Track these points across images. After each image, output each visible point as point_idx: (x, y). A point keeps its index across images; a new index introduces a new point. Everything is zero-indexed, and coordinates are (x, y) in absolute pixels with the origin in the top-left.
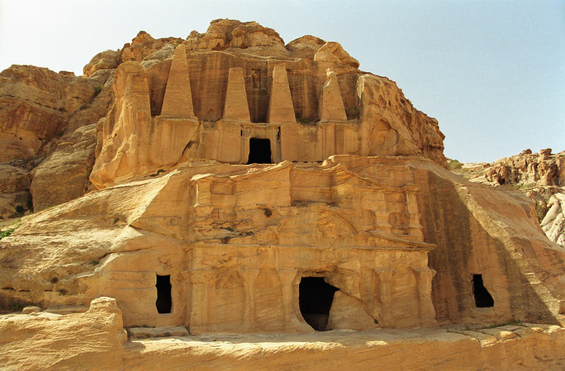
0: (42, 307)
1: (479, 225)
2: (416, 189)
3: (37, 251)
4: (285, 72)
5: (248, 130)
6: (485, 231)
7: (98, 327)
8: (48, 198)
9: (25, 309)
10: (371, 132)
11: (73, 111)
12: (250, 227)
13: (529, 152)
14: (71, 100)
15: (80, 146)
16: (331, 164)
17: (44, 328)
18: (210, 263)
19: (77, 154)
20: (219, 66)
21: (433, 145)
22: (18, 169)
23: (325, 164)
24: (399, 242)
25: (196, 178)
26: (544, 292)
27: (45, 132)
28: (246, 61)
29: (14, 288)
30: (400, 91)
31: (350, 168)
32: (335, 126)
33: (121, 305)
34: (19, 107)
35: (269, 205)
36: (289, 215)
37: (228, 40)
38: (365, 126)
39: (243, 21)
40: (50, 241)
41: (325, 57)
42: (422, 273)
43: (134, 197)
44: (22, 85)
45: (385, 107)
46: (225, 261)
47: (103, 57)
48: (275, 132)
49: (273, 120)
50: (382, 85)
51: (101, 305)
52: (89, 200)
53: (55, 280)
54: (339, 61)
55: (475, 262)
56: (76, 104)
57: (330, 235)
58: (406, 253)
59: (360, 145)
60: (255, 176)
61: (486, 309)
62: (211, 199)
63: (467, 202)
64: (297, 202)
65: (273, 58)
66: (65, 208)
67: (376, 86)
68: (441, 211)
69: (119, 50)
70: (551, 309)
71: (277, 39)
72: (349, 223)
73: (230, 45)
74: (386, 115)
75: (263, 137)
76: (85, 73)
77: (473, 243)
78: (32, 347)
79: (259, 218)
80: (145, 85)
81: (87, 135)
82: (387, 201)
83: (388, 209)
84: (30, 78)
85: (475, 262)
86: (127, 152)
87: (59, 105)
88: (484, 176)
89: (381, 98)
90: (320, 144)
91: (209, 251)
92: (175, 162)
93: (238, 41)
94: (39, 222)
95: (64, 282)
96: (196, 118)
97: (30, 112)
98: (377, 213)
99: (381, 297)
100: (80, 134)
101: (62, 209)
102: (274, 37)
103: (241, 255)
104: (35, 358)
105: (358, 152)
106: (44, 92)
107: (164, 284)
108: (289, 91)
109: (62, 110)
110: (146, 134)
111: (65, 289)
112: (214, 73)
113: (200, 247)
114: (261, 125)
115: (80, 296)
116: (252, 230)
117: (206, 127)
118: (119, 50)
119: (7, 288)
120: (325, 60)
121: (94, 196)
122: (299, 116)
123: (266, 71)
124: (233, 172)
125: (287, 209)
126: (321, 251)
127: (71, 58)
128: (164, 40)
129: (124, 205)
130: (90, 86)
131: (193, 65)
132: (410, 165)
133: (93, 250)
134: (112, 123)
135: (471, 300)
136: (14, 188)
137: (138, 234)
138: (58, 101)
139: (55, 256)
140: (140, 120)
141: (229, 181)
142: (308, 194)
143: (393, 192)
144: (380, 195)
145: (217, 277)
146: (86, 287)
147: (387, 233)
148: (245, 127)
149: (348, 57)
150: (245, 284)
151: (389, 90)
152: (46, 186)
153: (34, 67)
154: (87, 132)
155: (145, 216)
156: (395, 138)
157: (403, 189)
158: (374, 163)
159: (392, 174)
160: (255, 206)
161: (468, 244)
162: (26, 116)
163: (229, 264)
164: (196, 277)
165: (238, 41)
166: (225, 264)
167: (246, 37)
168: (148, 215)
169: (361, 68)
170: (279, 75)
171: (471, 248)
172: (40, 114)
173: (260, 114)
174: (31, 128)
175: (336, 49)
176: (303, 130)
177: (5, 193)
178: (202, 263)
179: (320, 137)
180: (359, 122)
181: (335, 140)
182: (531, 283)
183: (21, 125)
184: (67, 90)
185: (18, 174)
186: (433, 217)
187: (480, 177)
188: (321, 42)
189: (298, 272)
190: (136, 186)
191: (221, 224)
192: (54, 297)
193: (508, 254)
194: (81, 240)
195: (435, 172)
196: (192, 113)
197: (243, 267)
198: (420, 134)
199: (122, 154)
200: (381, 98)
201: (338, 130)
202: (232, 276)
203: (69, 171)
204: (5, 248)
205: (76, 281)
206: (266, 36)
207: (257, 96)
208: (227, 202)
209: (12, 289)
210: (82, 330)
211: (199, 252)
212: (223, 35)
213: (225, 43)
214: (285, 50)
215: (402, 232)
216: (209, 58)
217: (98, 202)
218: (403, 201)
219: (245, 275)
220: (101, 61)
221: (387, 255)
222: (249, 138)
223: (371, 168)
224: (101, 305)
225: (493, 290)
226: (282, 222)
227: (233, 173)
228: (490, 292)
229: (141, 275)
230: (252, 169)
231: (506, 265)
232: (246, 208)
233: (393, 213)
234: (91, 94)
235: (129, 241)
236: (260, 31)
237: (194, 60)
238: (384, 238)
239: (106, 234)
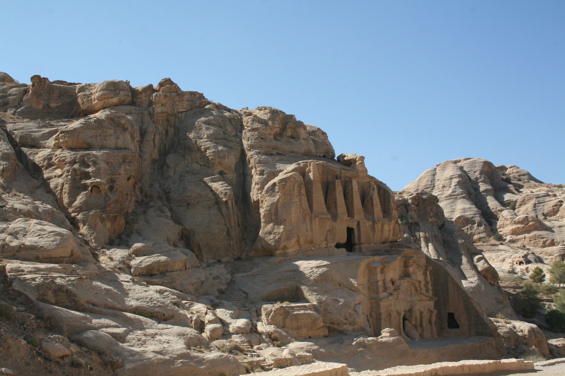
48: (356, 223)
49: (357, 217)
59: (389, 234)
93: (289, 132)
103: (391, 305)
110: (309, 224)
165: (289, 132)
173: (350, 213)
179: (376, 229)
201: (383, 225)
211: (382, 303)
219: (392, 314)
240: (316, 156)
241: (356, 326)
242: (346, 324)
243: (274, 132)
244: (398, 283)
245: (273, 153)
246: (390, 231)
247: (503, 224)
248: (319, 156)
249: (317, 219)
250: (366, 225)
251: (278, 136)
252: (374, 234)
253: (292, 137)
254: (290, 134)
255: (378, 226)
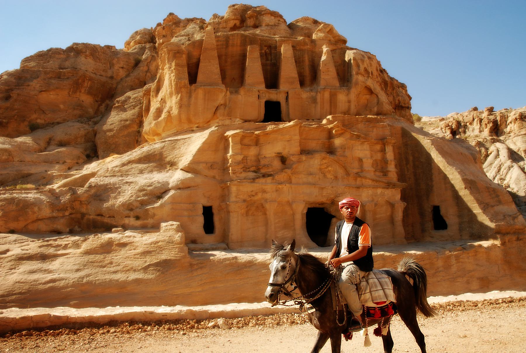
0: (125, 228)
2: (393, 141)
3: (117, 188)
4: (291, 49)
5: (264, 95)
7: (170, 242)
9: (113, 230)
10: (358, 96)
11: (119, 79)
12: (270, 170)
13: (475, 109)
14: (118, 70)
15: (130, 107)
16: (330, 122)
17: (133, 242)
18: (241, 197)
19: (129, 114)
20: (239, 44)
21: (403, 105)
22: (85, 126)
23: (324, 122)
24: (380, 182)
25: (229, 133)
27: (100, 96)
28: (260, 39)
29: (104, 215)
30: (379, 63)
31: (344, 125)
32: (330, 92)
33: (182, 228)
34: (81, 76)
35: (285, 153)
36: (299, 161)
37: (243, 21)
38: (354, 92)
39: (254, 5)
40: (125, 181)
42: (396, 205)
43: (182, 148)
44: (82, 59)
45: (368, 77)
46: (253, 196)
47: (140, 34)
49: (283, 86)
50: (366, 59)
51: (170, 227)
52: (149, 150)
53: (131, 210)
54: (332, 39)
56: (122, 73)
57: (329, 176)
58: (385, 190)
60: (273, 132)
61: (441, 231)
62: (242, 149)
64: (305, 152)
65: (281, 37)
66: (131, 156)
67: (361, 60)
68: (411, 158)
69: (152, 28)
71: (281, 20)
72: (344, 167)
73: (245, 25)
74: (370, 83)
75: (275, 100)
76: (125, 47)
78: (127, 255)
79: (277, 164)
80: (184, 59)
81: (135, 98)
82: (371, 151)
83: (372, 157)
84: (87, 53)
86: (171, 113)
87: (110, 73)
88: (440, 128)
89: (366, 70)
90: (319, 106)
91: (241, 188)
92: (208, 120)
93: (250, 22)
94: (114, 167)
95: (138, 212)
96: (224, 85)
97: (89, 80)
98: (364, 160)
100: (129, 98)
101: (130, 157)
102: (279, 18)
103: (264, 191)
104: (131, 262)
105: (347, 112)
106: (98, 64)
107: (208, 212)
108: (294, 64)
109: (112, 78)
111: (141, 215)
112: (235, 50)
113: (234, 185)
114: (271, 91)
115: (150, 221)
116: (272, 173)
117: (231, 93)
118: (152, 28)
119: (98, 215)
121: (151, 147)
122: (302, 84)
123: (276, 47)
124: (256, 128)
125: (297, 156)
126: (322, 188)
127: (116, 36)
128: (189, 21)
129: (175, 154)
130: (131, 58)
131: (219, 43)
132: (388, 122)
133: (156, 188)
134: (158, 90)
135: (430, 224)
136: (83, 140)
137: (189, 175)
138: (109, 71)
139: (130, 192)
140: (181, 88)
141: (254, 136)
142: (313, 145)
143: (376, 143)
144: (366, 146)
145: (247, 207)
146: (154, 215)
147: (371, 175)
148: (261, 92)
149: (339, 36)
150: (268, 213)
151: (372, 62)
153: (89, 44)
154: (135, 96)
155: (193, 162)
156: (375, 101)
157: (383, 141)
158: (362, 121)
159: (375, 130)
160: (274, 155)
162: (86, 84)
163: (256, 198)
164: (233, 207)
166: (253, 198)
167: (257, 18)
168: (195, 161)
169: (348, 44)
170: (285, 50)
172: (96, 82)
174: (89, 93)
175: (330, 30)
176: (305, 94)
177: (77, 144)
178: (236, 197)
179: (319, 100)
180: (349, 89)
181: (331, 102)
183: (83, 91)
184: (115, 62)
185: (85, 130)
186: (405, 163)
187: (437, 129)
188: (316, 22)
189: (306, 203)
190: (183, 139)
191: (249, 168)
192: (132, 221)
194: (146, 181)
195: (407, 128)
196: (220, 82)
197: (266, 200)
198: (394, 97)
199: (167, 114)
200: (366, 70)
202: (257, 207)
203: (123, 126)
204: (95, 186)
205: (147, 210)
206: (273, 17)
207: (269, 68)
208: (253, 152)
209: (102, 215)
210: (160, 244)
212: (239, 17)
213: (240, 24)
214: (288, 29)
215: (382, 174)
216: (231, 38)
217: (155, 152)
218: (383, 151)
219: (267, 206)
220: (138, 38)
221: (370, 192)
222: (264, 100)
223: (359, 125)
224: (170, 227)
226: (294, 166)
227: (257, 129)
228: (445, 219)
229: (191, 205)
230: (270, 127)
232: (267, 156)
233: (376, 160)
234: (132, 65)
235: (183, 181)
236: (268, 14)
237: (220, 39)
238: (369, 179)
239: (164, 176)
242: (128, 217)
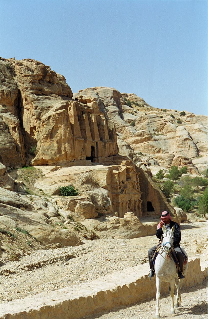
1: (152, 187)
6: (154, 189)
8: (9, 161)
26: (170, 208)
41: (96, 106)
48: (96, 143)
55: (150, 198)
59: (113, 151)
63: (148, 178)
70: (172, 212)
77: (149, 192)
85: (150, 198)
93: (48, 79)
99: (136, 209)
120: (96, 108)
152: (7, 154)
161: (147, 192)
165: (48, 79)
167: (51, 78)
171: (148, 193)
182: (167, 205)
193: (161, 196)
201: (110, 145)
225: (155, 207)
231: (160, 199)
240: (63, 95)
241: (109, 211)
243: (39, 78)
244: (126, 182)
245: (39, 93)
246: (113, 148)
247: (127, 137)
248: (65, 96)
249: (77, 141)
250: (101, 144)
251: (41, 81)
252: (105, 151)
253: (49, 82)
254: (49, 80)
255: (107, 146)
